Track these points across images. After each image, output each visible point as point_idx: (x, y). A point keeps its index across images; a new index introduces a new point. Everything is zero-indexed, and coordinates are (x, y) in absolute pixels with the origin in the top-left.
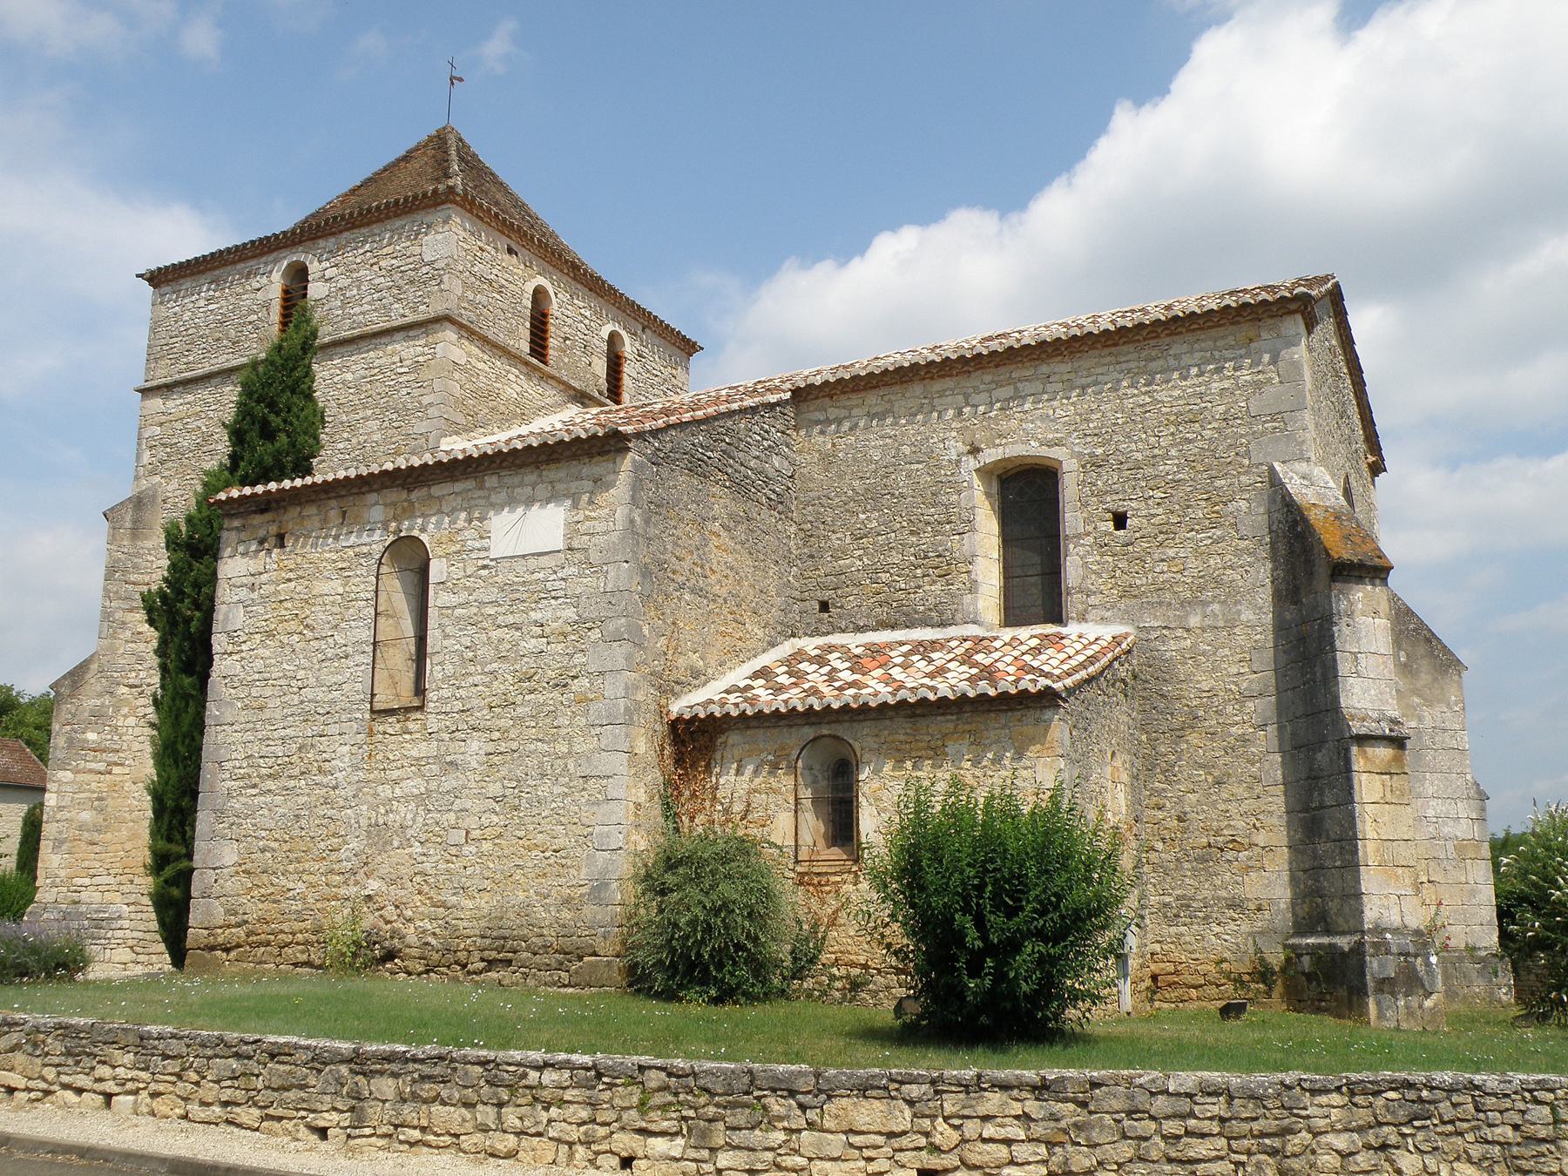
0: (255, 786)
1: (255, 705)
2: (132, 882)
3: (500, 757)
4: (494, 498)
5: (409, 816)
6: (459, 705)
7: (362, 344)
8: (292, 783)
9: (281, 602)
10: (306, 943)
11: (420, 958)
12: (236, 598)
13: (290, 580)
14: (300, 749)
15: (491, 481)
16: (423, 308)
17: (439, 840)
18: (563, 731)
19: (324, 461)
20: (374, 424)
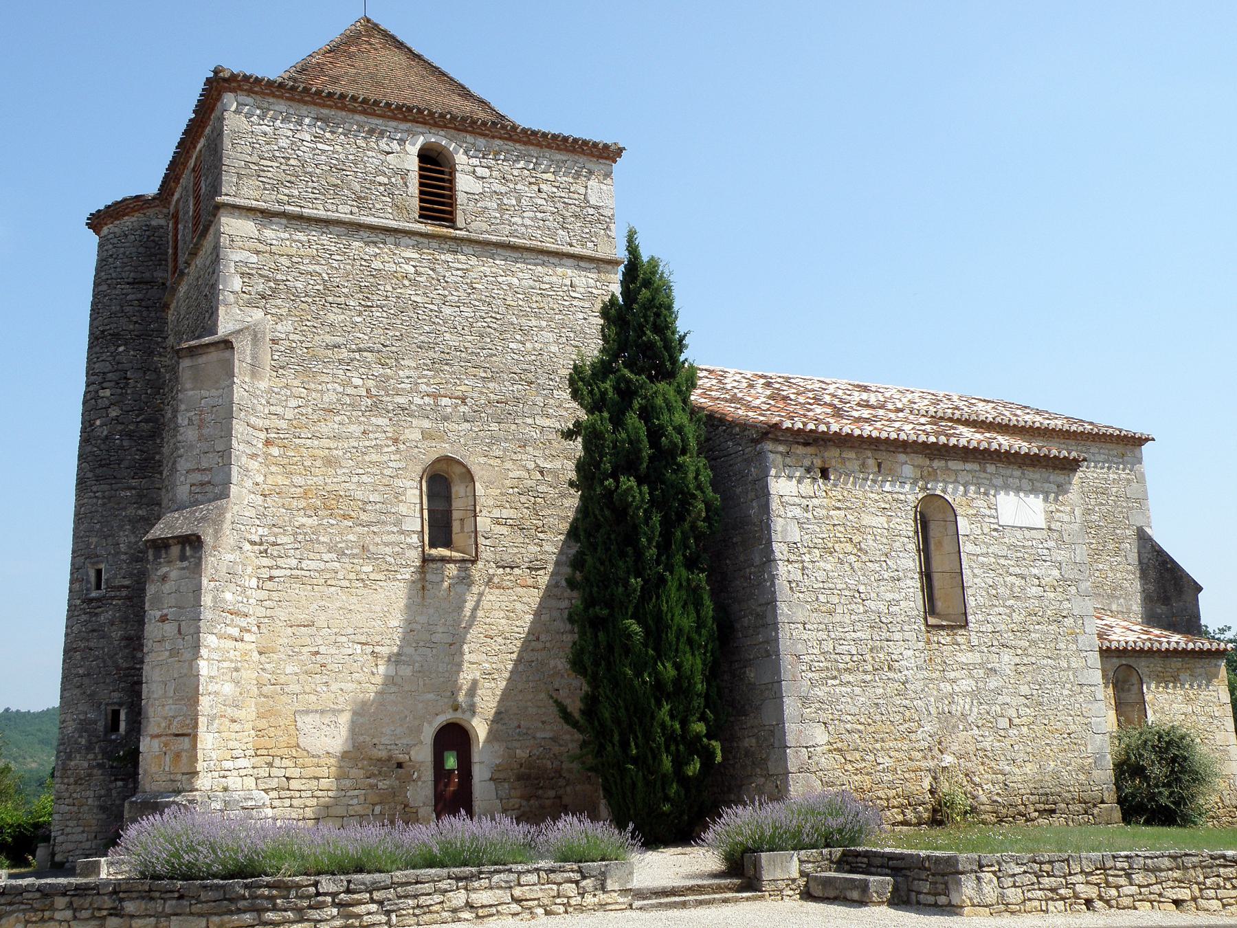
0: (835, 678)
1: (823, 609)
2: (270, 765)
3: (1024, 668)
4: (994, 481)
5: (967, 707)
6: (990, 628)
7: (526, 255)
8: (868, 678)
9: (834, 525)
10: (901, 806)
11: (992, 812)
12: (790, 515)
13: (839, 509)
14: (871, 650)
15: (991, 468)
16: (590, 245)
17: (990, 725)
18: (1063, 653)
19: (496, 355)
20: (551, 337)
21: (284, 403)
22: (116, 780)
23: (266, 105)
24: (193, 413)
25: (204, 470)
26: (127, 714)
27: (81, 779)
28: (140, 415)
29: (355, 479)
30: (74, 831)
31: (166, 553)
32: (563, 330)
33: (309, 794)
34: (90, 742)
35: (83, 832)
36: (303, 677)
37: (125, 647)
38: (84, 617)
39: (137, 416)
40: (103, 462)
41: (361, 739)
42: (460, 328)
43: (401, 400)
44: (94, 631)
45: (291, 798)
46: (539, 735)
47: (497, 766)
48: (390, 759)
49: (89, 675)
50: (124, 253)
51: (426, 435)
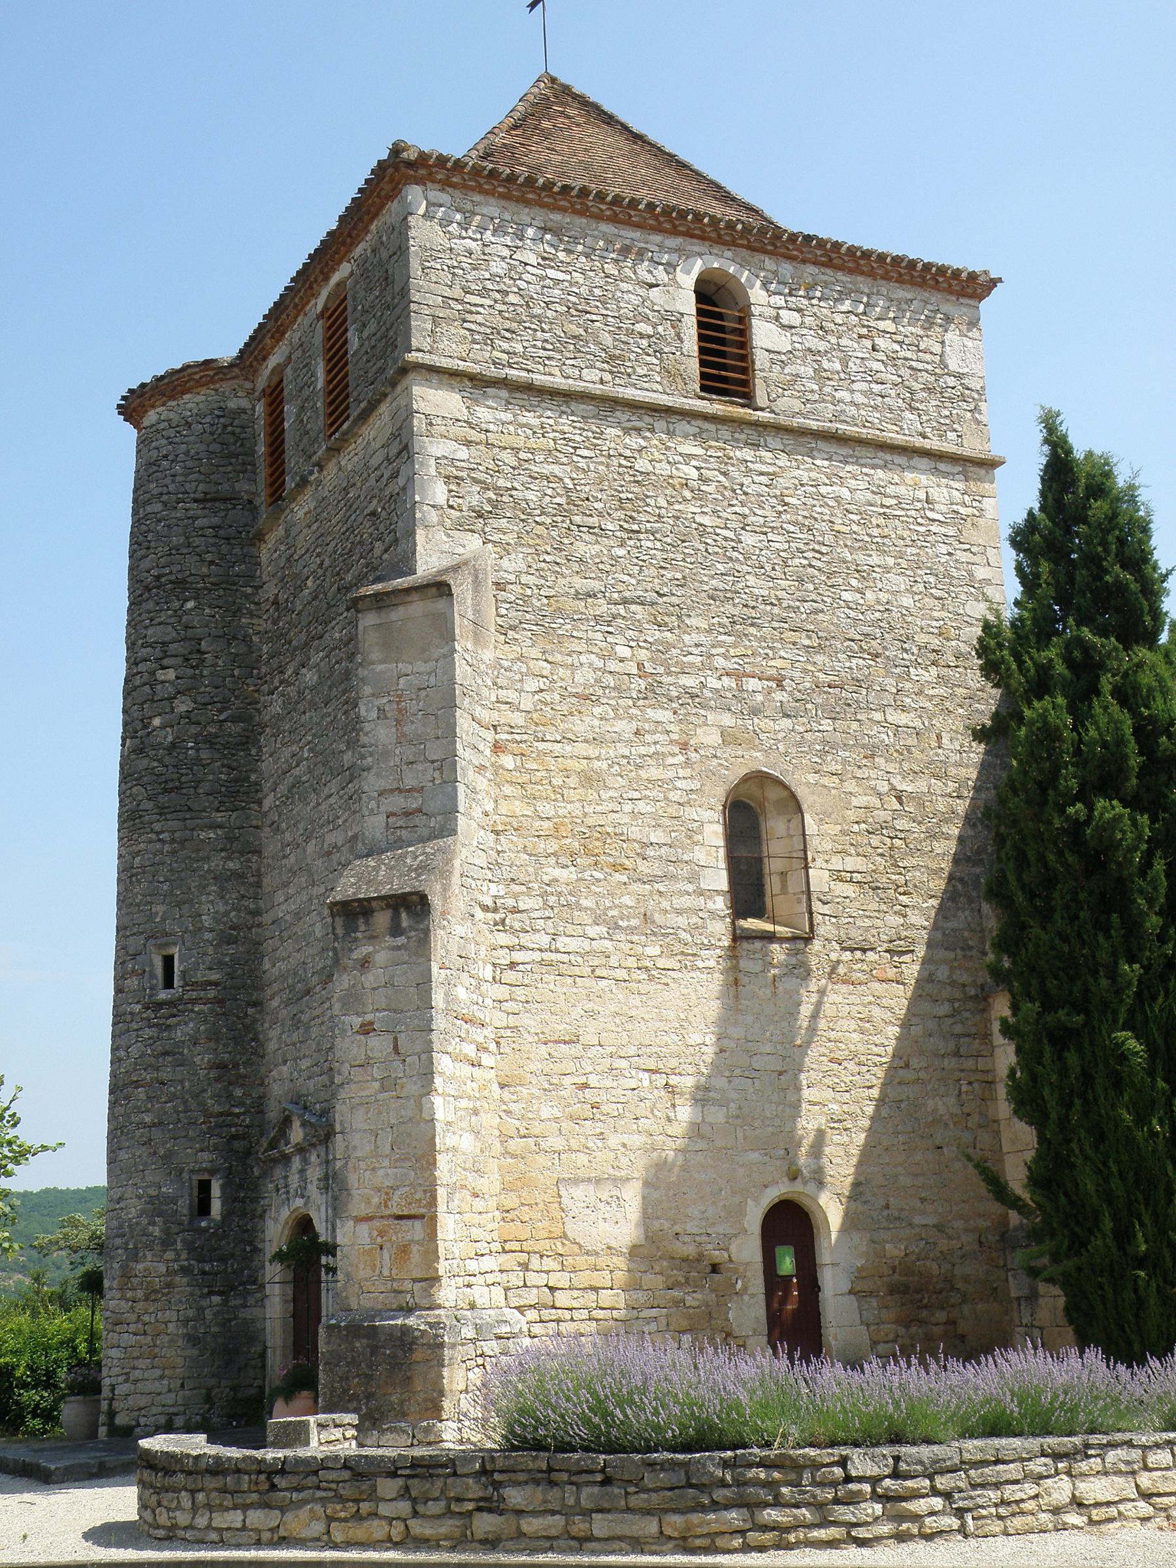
2: (525, 1267)
7: (860, 451)
16: (951, 435)
19: (822, 611)
20: (901, 582)
21: (518, 686)
22: (211, 1293)
23: (469, 206)
24: (385, 700)
25: (409, 791)
26: (223, 1187)
27: (155, 1291)
28: (226, 709)
29: (628, 807)
30: (146, 1376)
31: (367, 923)
32: (919, 572)
33: (584, 1314)
34: (167, 1232)
35: (162, 1377)
36: (566, 1125)
37: (218, 1079)
38: (148, 1033)
39: (220, 711)
40: (170, 785)
41: (657, 1225)
42: (768, 567)
43: (689, 681)
44: (166, 1053)
45: (558, 1321)
46: (918, 1220)
47: (860, 1270)
48: (700, 1258)
49: (161, 1124)
50: (187, 453)
51: (728, 738)
